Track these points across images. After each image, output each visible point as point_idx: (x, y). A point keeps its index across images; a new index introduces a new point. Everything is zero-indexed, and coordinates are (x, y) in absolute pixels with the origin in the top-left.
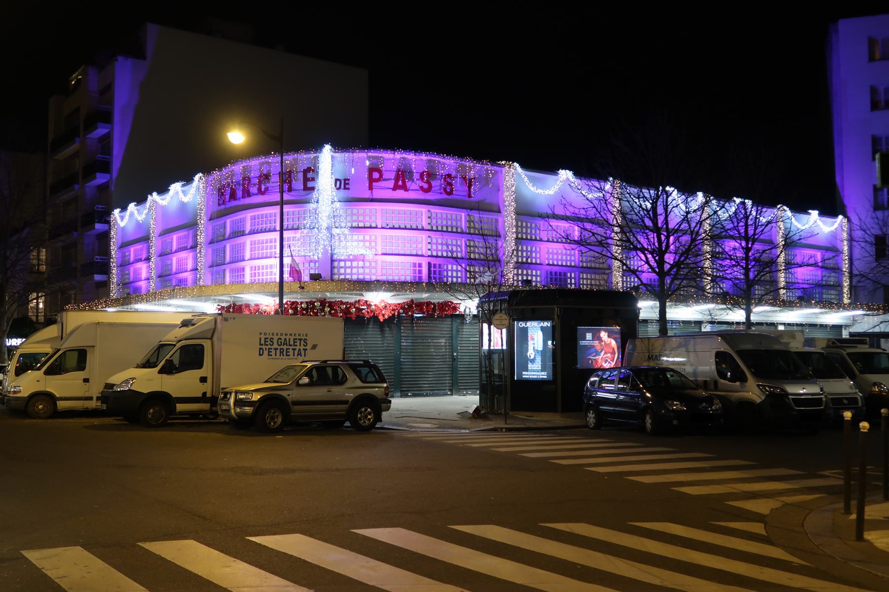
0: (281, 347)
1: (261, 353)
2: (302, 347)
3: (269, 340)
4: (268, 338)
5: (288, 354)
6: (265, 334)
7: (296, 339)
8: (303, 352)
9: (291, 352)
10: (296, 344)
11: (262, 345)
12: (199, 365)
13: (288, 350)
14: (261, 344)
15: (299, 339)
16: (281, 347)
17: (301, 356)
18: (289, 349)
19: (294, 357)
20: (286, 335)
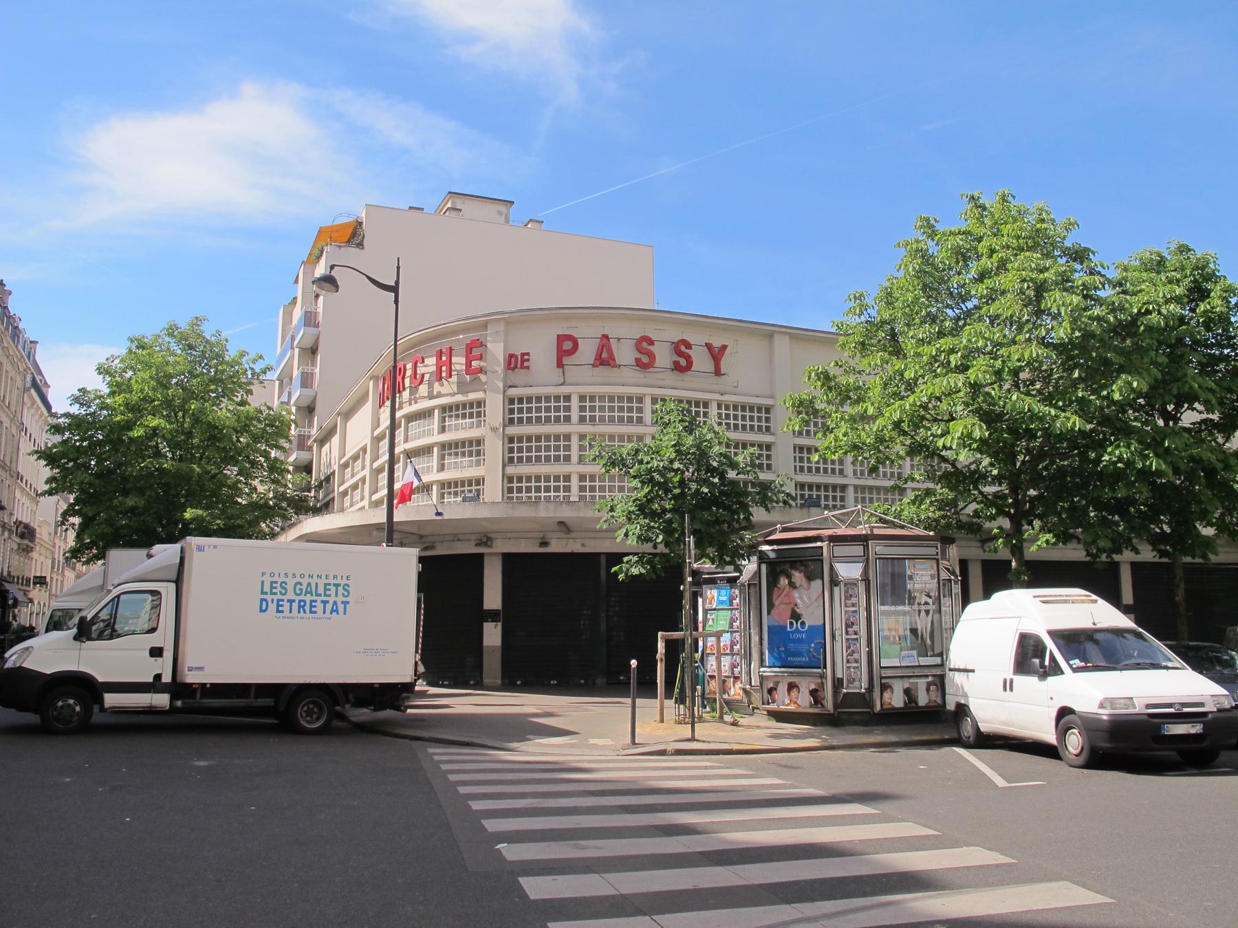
1: (264, 608)
2: (340, 599)
3: (278, 585)
4: (276, 582)
5: (313, 609)
6: (273, 574)
7: (330, 584)
8: (341, 607)
9: (320, 607)
10: (328, 592)
11: (266, 593)
14: (263, 593)
17: (338, 614)
18: (316, 601)
20: (311, 576)
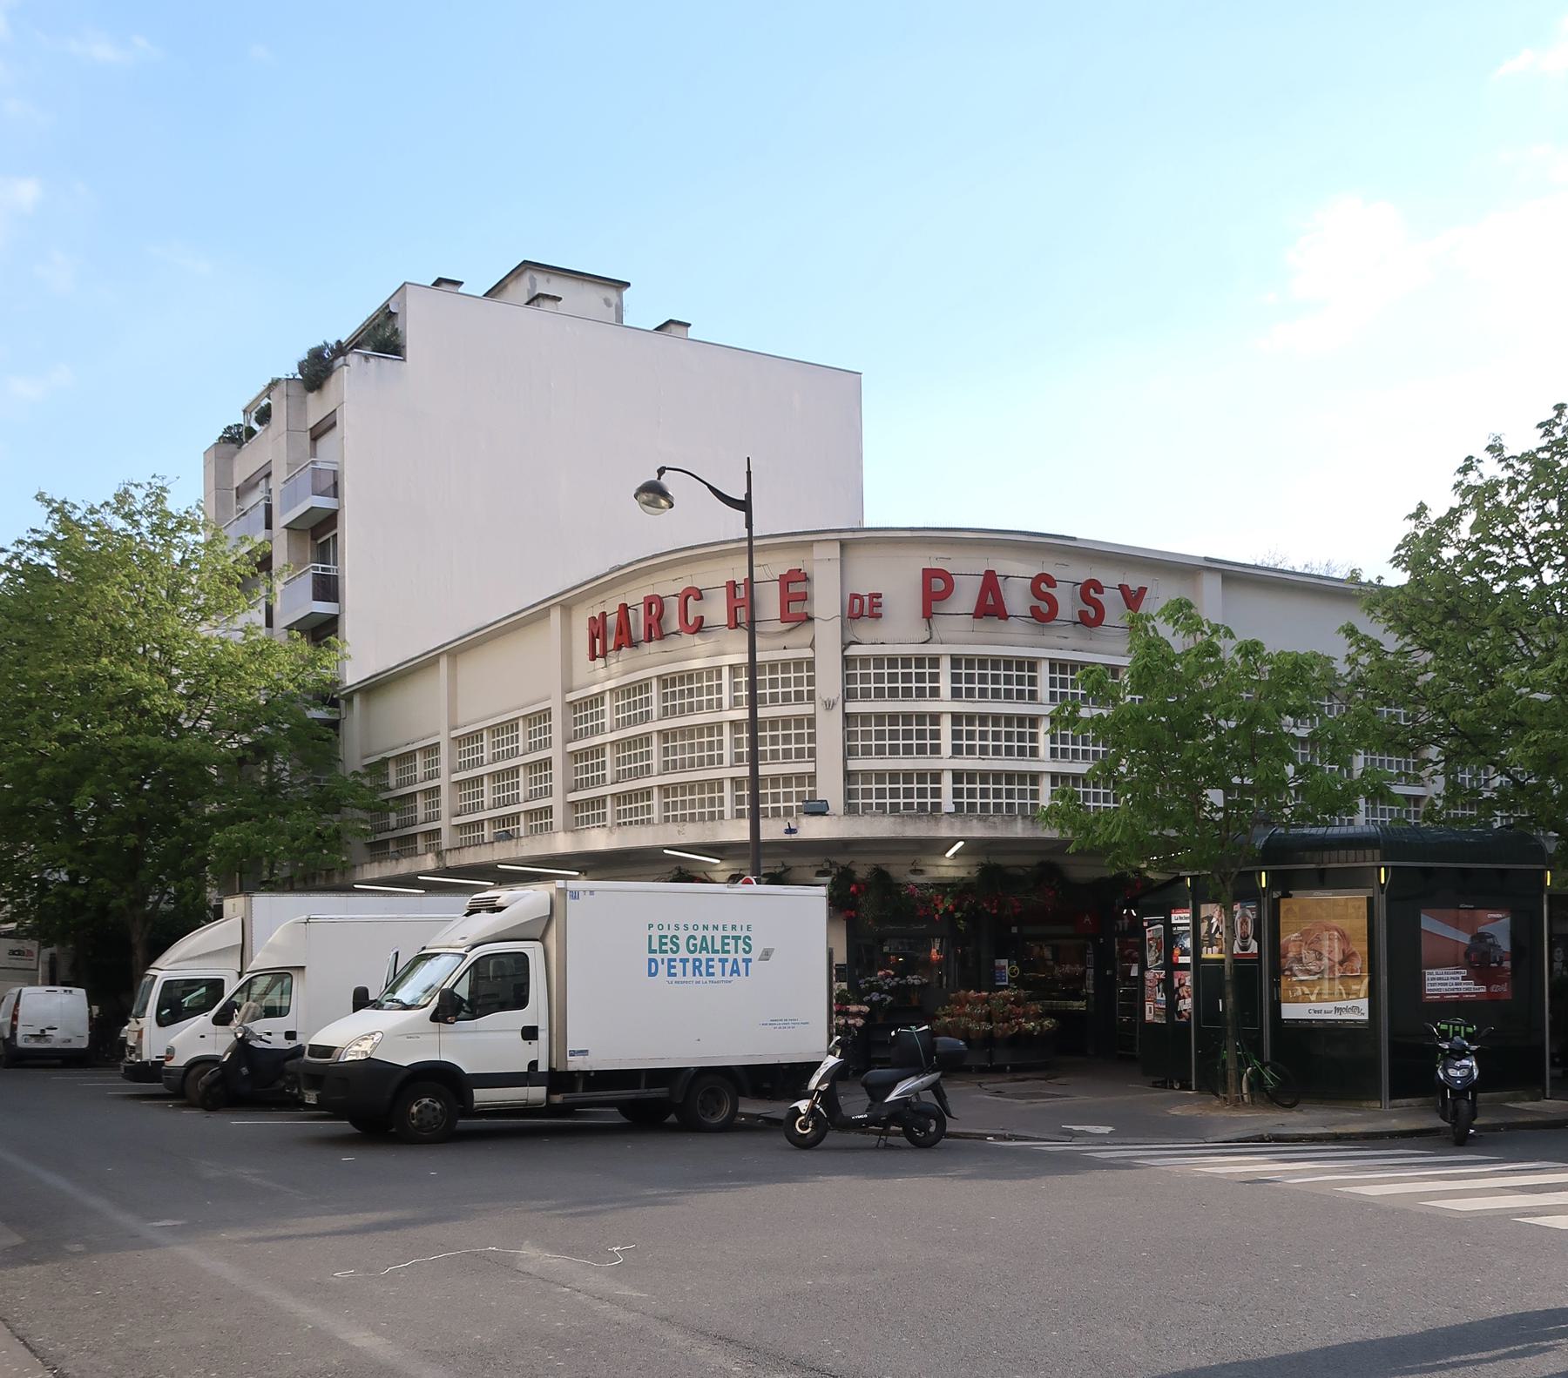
0: (696, 955)
1: (653, 971)
2: (741, 956)
3: (668, 941)
4: (666, 937)
5: (711, 970)
6: (660, 927)
7: (728, 937)
8: (742, 966)
9: (718, 966)
10: (726, 948)
11: (655, 951)
12: (519, 1000)
13: (711, 963)
14: (652, 951)
15: (734, 938)
16: (696, 955)
17: (739, 975)
18: (713, 960)
19: (723, 978)
20: (706, 928)
